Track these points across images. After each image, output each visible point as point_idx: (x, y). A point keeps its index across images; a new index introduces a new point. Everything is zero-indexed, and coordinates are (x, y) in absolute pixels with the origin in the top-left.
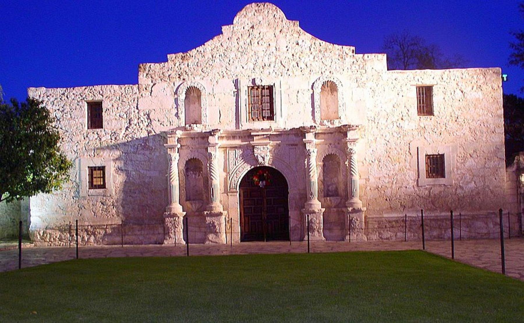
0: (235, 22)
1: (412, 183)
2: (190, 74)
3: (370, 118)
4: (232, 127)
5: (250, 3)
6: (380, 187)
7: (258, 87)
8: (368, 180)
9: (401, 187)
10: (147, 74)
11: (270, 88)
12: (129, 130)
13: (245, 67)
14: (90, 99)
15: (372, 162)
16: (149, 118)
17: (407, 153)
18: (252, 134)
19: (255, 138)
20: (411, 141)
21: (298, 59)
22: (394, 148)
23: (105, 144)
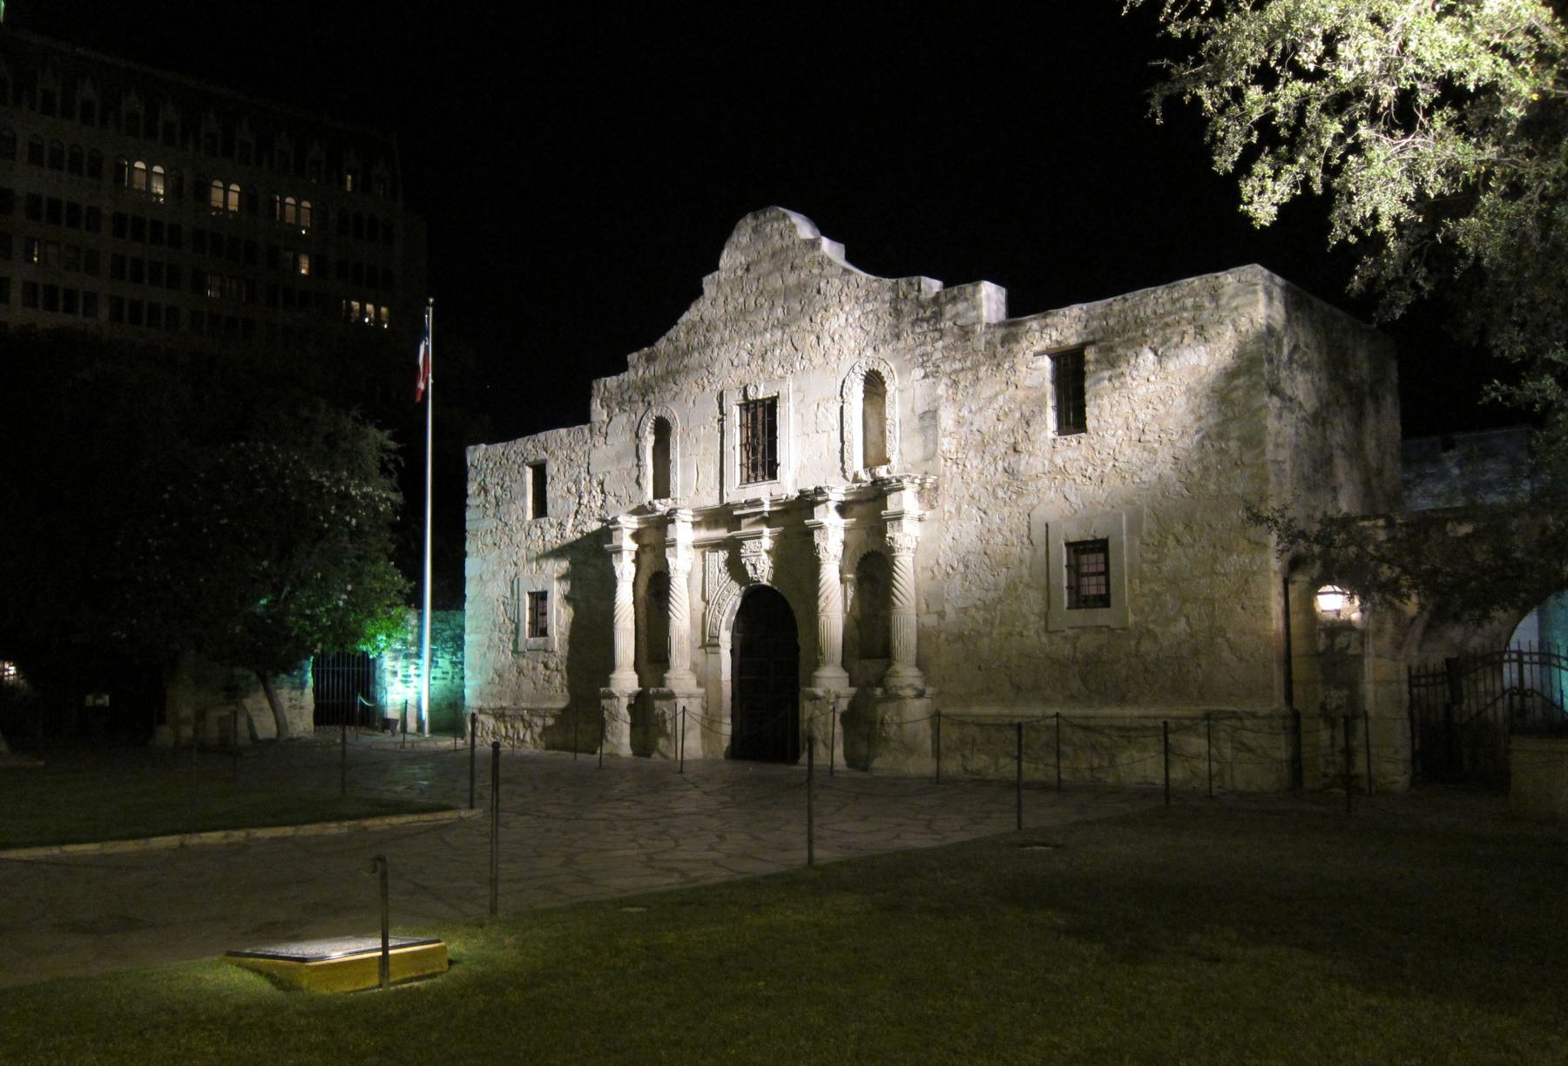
0: (722, 263)
1: (1035, 623)
2: (656, 390)
3: (948, 455)
4: (712, 501)
5: (742, 215)
6: (966, 633)
7: (756, 402)
8: (941, 614)
9: (1010, 634)
10: (601, 401)
11: (771, 405)
12: (579, 517)
13: (735, 363)
14: (531, 459)
15: (953, 568)
16: (603, 492)
17: (1025, 540)
18: (736, 513)
19: (744, 522)
20: (1033, 508)
21: (818, 328)
22: (996, 530)
23: (549, 547)
